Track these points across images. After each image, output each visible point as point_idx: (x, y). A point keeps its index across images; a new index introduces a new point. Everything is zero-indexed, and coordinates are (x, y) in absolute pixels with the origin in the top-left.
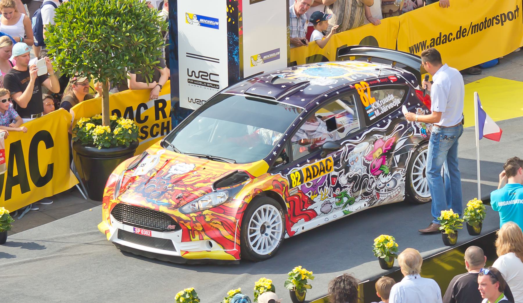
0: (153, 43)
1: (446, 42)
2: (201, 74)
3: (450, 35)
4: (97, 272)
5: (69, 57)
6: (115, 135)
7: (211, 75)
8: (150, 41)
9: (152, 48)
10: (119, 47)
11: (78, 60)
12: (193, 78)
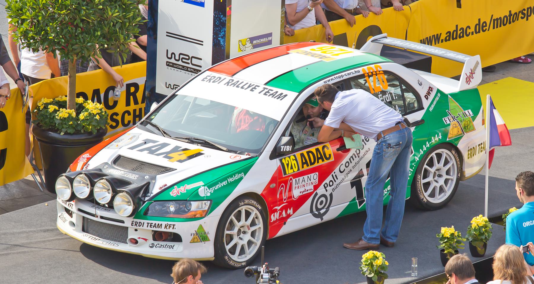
0: (129, 19)
1: (463, 36)
2: (181, 56)
3: (468, 28)
4: (47, 275)
5: (33, 29)
6: (81, 120)
7: (193, 59)
8: (126, 16)
9: (128, 24)
10: (90, 21)
11: (43, 33)
12: (173, 61)
